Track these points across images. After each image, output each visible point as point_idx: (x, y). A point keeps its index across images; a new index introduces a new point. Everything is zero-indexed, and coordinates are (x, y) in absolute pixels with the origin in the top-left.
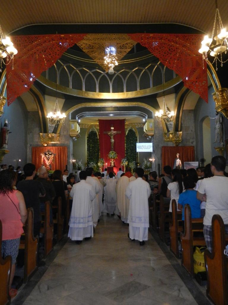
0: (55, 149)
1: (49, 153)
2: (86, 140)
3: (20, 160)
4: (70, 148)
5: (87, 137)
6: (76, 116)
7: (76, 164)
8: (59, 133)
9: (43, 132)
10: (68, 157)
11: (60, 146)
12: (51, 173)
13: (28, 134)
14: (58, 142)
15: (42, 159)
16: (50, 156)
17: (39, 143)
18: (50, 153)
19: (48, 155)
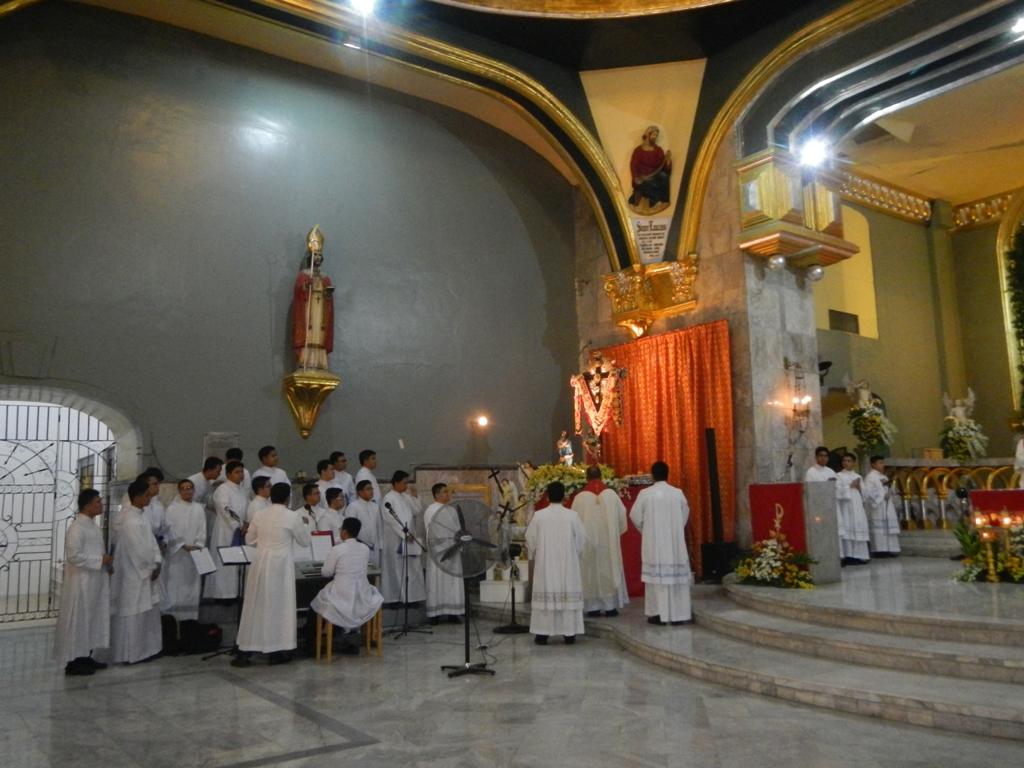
0: (675, 347)
1: (598, 370)
2: (1003, 274)
3: (483, 421)
4: (747, 329)
5: (1010, 255)
6: (770, 127)
7: (881, 419)
8: (689, 253)
9: (619, 267)
10: (739, 380)
11: (704, 324)
12: (577, 481)
13: (577, 293)
14: (690, 305)
15: (576, 406)
16: (604, 382)
17: (617, 329)
18: (603, 371)
19: (596, 379)
